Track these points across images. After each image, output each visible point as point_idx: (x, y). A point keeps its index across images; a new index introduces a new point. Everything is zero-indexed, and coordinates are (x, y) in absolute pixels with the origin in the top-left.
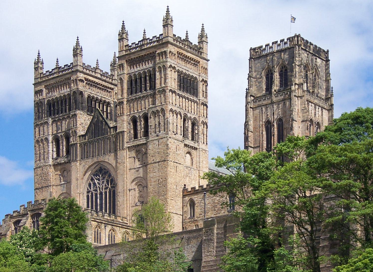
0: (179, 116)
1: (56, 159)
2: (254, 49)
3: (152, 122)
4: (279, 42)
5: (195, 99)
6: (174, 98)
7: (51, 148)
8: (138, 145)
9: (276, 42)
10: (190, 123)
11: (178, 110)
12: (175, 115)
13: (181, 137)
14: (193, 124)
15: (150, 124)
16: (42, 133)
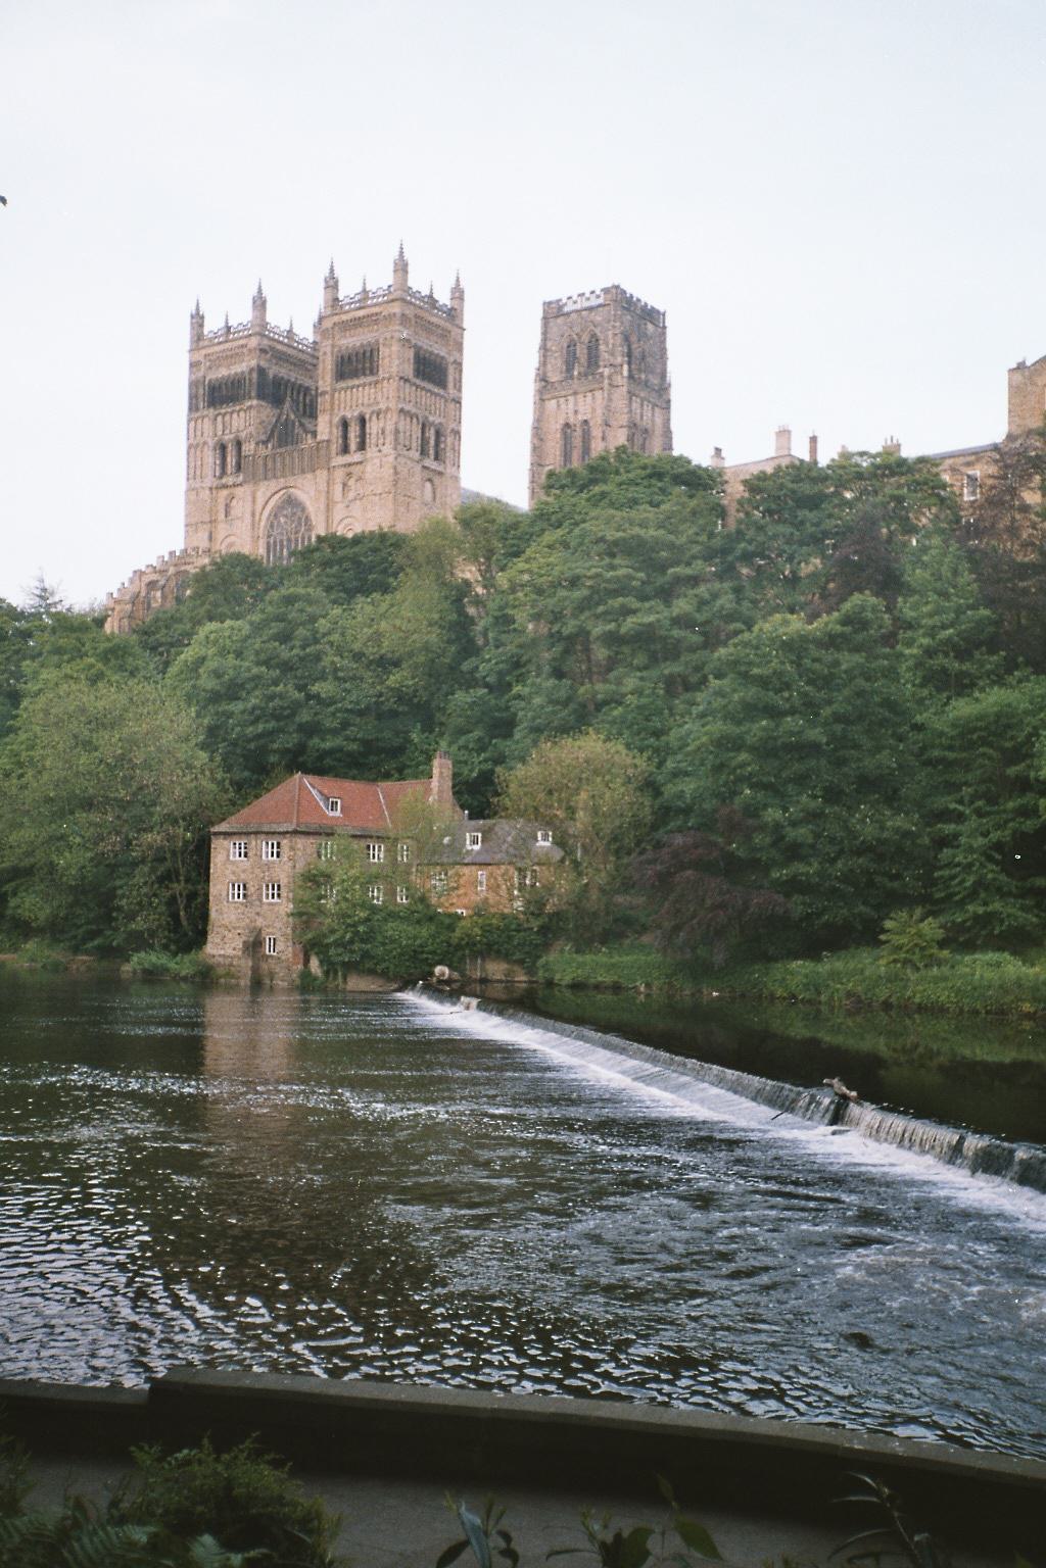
0: (415, 420)
1: (221, 477)
2: (550, 303)
3: (373, 427)
4: (587, 295)
5: (442, 392)
6: (407, 390)
7: (210, 458)
8: (350, 465)
9: (583, 294)
10: (432, 431)
11: (414, 410)
12: (408, 419)
13: (416, 455)
14: (438, 434)
15: (368, 431)
16: (199, 433)
